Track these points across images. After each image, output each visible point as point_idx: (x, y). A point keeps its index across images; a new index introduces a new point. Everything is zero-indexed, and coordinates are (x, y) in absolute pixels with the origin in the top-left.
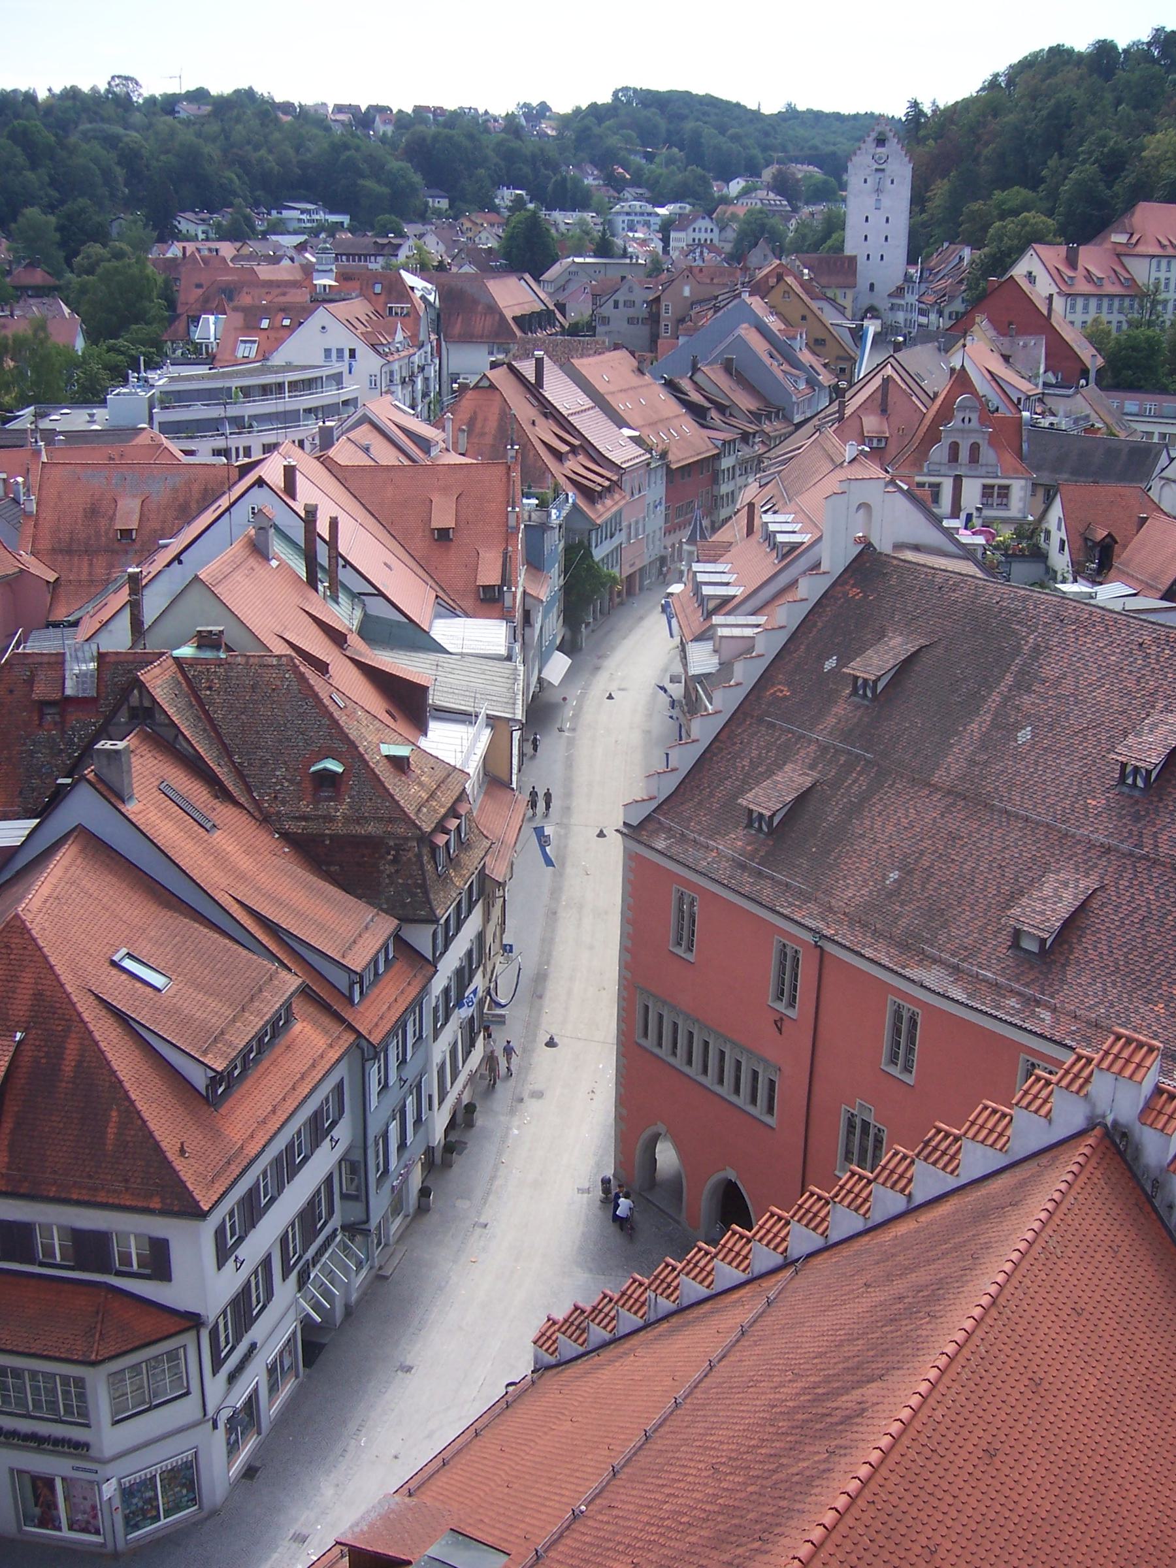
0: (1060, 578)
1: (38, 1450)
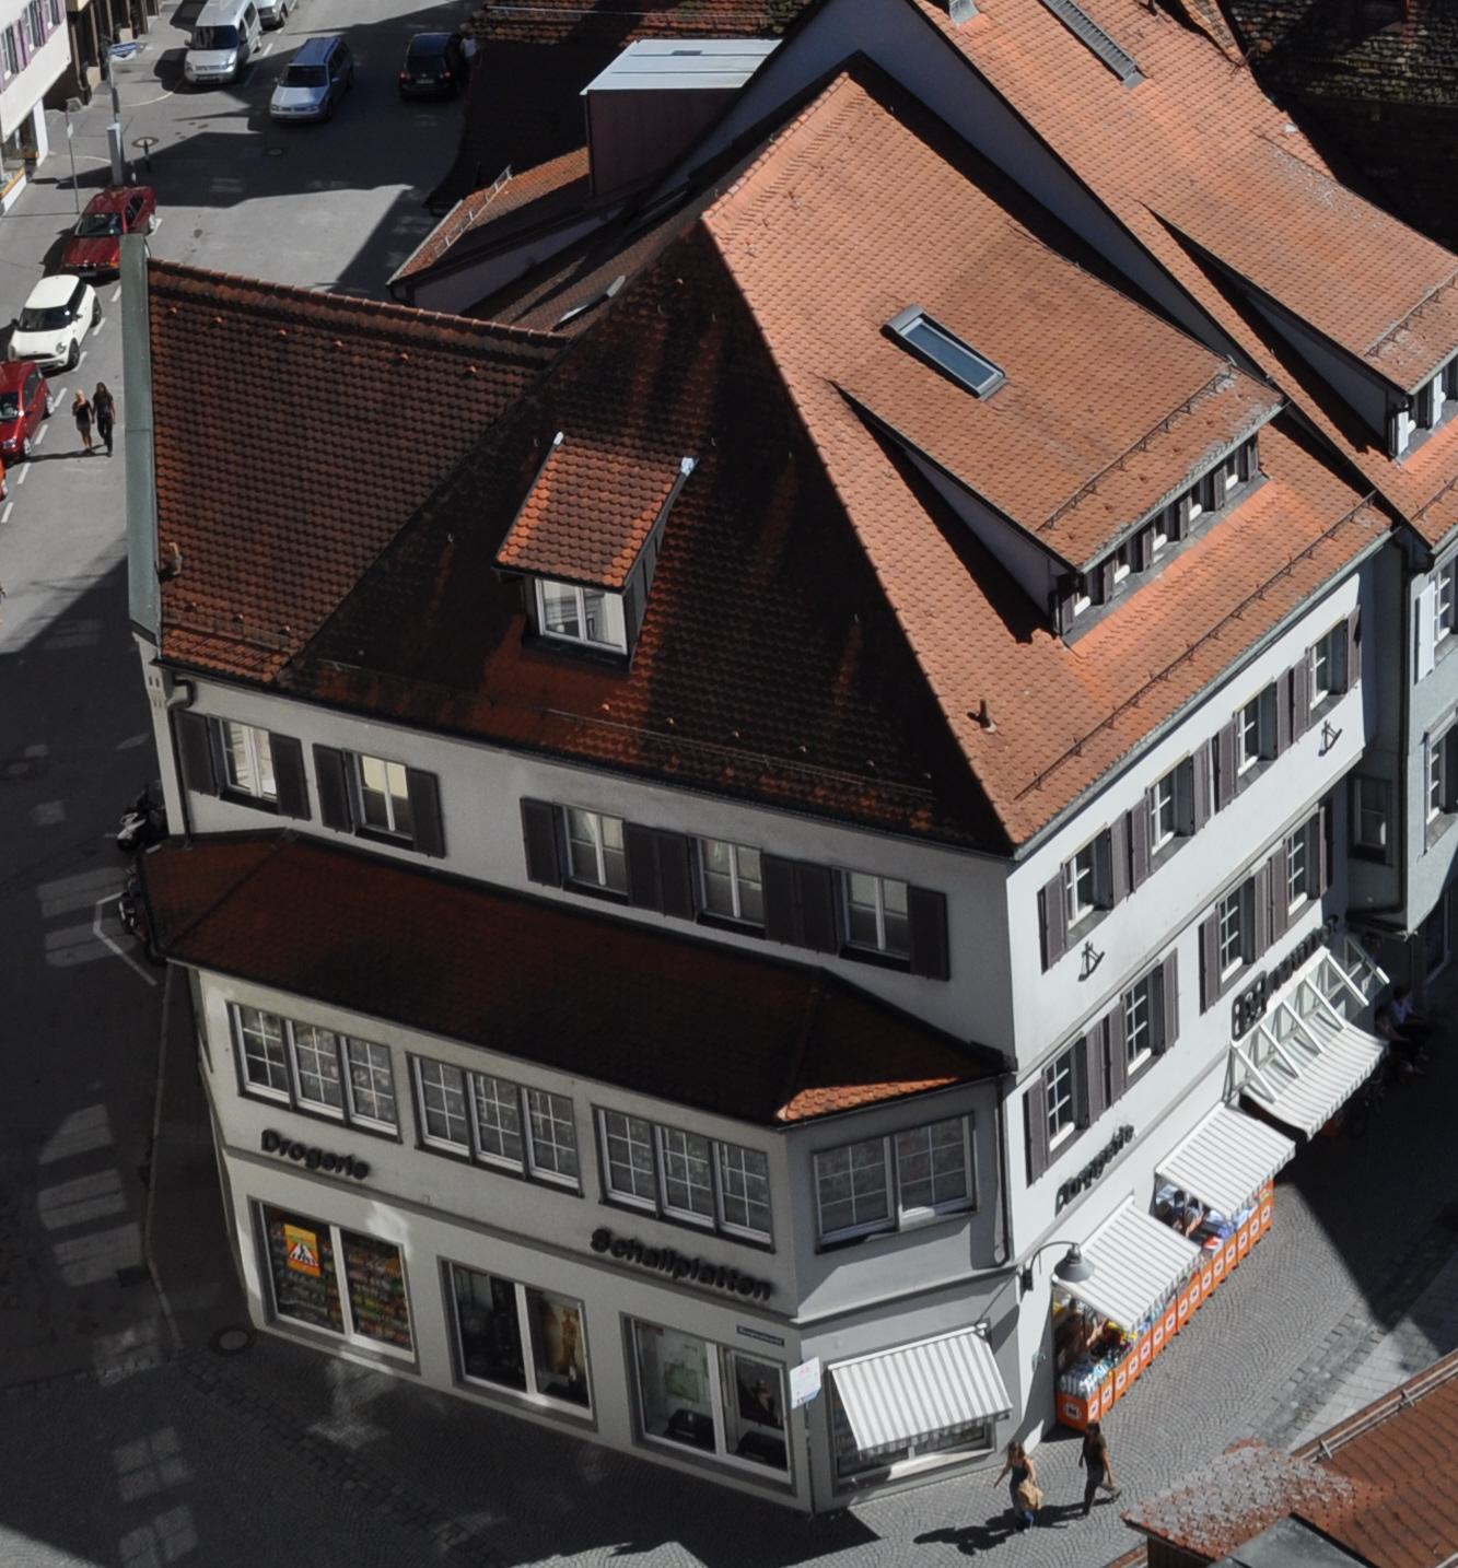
1: (673, 1285)
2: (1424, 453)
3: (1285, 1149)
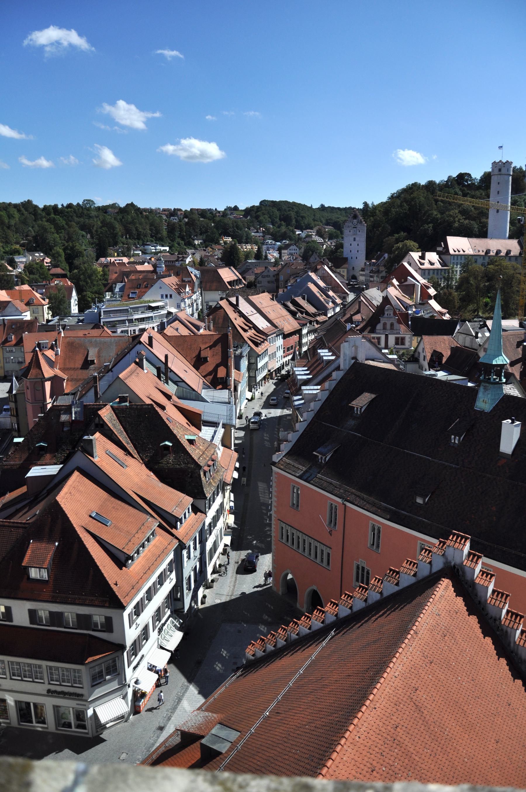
0: (424, 369)
2: (182, 528)
3: (169, 655)
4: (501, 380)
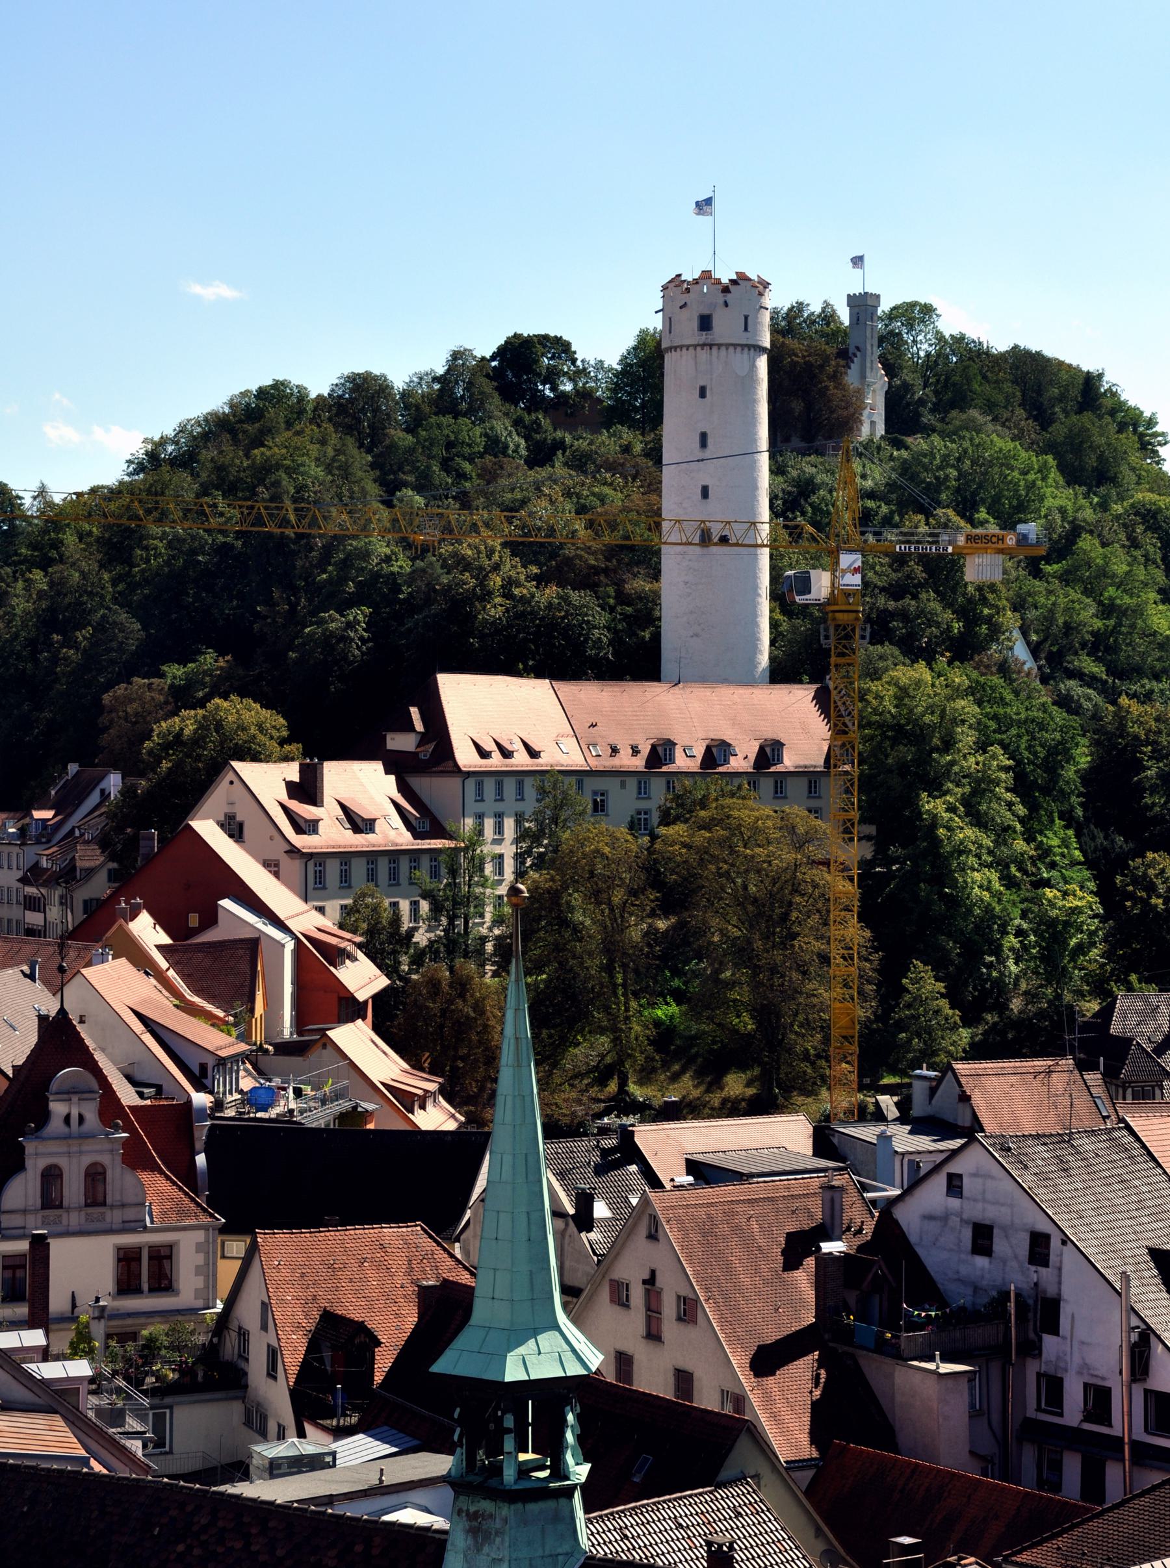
0: (272, 1427)
4: (559, 1472)
